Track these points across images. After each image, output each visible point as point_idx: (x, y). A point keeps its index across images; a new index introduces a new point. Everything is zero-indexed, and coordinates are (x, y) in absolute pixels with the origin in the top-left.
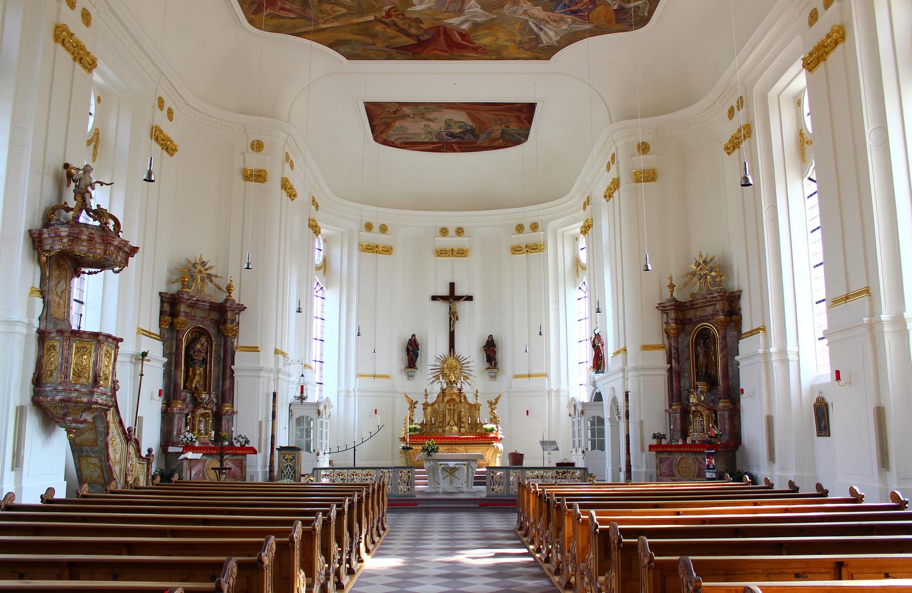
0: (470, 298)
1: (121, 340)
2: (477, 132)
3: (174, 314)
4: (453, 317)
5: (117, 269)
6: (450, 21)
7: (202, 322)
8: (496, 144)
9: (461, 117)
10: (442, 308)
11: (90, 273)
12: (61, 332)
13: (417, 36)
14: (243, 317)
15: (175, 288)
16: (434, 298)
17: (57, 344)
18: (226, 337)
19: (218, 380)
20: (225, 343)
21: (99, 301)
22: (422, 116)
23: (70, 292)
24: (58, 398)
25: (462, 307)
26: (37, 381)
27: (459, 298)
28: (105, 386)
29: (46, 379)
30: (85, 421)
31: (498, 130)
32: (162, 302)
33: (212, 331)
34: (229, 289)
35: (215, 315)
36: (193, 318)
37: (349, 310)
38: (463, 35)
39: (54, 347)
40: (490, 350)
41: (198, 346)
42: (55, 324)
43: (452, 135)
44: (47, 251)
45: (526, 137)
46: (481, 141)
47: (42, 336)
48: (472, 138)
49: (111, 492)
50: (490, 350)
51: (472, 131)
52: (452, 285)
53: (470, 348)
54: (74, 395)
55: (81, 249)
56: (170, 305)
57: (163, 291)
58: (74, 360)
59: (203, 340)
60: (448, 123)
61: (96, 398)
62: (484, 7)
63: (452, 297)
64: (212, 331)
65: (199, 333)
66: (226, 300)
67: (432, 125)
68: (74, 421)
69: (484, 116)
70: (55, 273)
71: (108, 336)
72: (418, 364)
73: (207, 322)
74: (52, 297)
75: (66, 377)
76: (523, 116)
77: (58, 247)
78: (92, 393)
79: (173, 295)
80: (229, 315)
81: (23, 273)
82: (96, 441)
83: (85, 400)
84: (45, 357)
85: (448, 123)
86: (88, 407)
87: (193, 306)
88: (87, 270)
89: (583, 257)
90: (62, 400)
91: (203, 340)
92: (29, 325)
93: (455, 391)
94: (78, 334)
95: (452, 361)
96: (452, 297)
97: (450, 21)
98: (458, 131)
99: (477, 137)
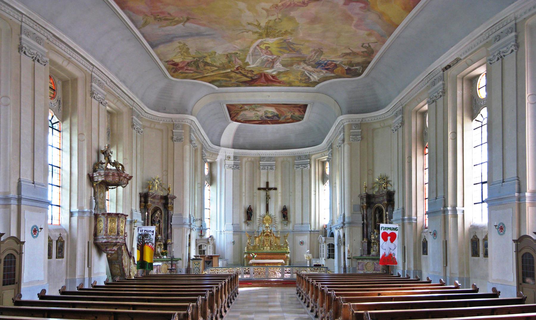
0: (275, 189)
1: (127, 216)
2: (279, 116)
3: (146, 202)
4: (268, 198)
5: (124, 186)
6: (267, 71)
7: (158, 204)
8: (289, 121)
9: (272, 110)
10: (263, 193)
11: (112, 188)
12: (103, 214)
13: (251, 77)
14: (175, 202)
15: (145, 190)
16: (259, 189)
17: (102, 219)
18: (168, 211)
19: (165, 229)
20: (168, 213)
21: (115, 200)
22: (254, 109)
23: (105, 197)
24: (104, 241)
25: (272, 192)
26: (95, 235)
27: (271, 189)
28: (122, 235)
29: (98, 234)
30: (114, 250)
31: (289, 115)
32: (141, 197)
33: (162, 208)
34: (169, 189)
35: (163, 201)
36: (154, 203)
37: (220, 195)
38: (273, 77)
39: (101, 221)
40: (285, 213)
41: (157, 215)
42: (101, 211)
43: (268, 117)
44: (97, 182)
45: (303, 118)
46: (282, 119)
47: (96, 216)
48: (277, 118)
49: (128, 280)
50: (285, 213)
51: (277, 116)
52: (267, 183)
53: (275, 211)
54: (110, 240)
55: (110, 179)
56: (144, 198)
57: (141, 192)
58: (109, 225)
59: (158, 212)
60: (266, 112)
61: (118, 240)
62: (283, 65)
63: (267, 188)
64: (162, 208)
65: (156, 210)
66: (168, 194)
67: (258, 113)
68: (110, 250)
69: (283, 109)
70: (99, 190)
71: (122, 214)
72: (252, 218)
73: (160, 204)
74: (99, 200)
75: (106, 232)
76: (301, 110)
77: (100, 179)
78: (117, 239)
79: (145, 194)
80: (170, 201)
81: (88, 191)
82: (118, 258)
83: (114, 241)
84: (98, 225)
85: (266, 112)
86: (115, 244)
87: (154, 197)
88: (111, 187)
89: (328, 172)
90: (105, 242)
91: (158, 212)
92: (91, 212)
93: (269, 231)
94: (110, 214)
95: (267, 217)
96: (267, 188)
97: (267, 71)
98: (271, 115)
99: (279, 118)
